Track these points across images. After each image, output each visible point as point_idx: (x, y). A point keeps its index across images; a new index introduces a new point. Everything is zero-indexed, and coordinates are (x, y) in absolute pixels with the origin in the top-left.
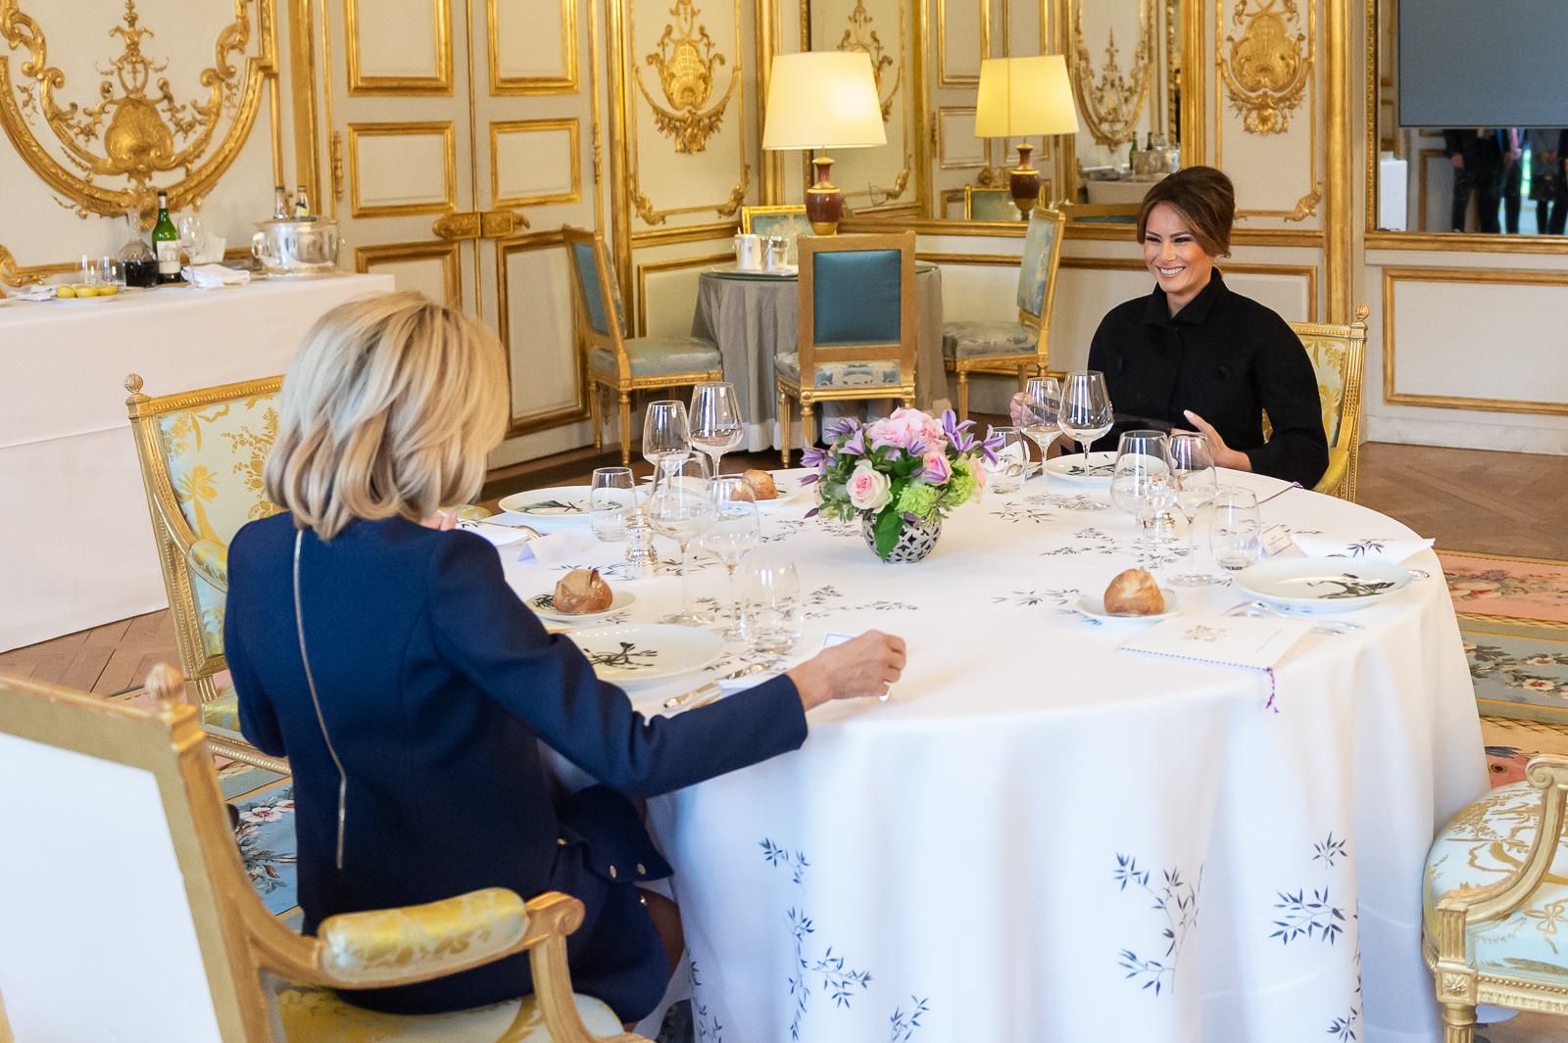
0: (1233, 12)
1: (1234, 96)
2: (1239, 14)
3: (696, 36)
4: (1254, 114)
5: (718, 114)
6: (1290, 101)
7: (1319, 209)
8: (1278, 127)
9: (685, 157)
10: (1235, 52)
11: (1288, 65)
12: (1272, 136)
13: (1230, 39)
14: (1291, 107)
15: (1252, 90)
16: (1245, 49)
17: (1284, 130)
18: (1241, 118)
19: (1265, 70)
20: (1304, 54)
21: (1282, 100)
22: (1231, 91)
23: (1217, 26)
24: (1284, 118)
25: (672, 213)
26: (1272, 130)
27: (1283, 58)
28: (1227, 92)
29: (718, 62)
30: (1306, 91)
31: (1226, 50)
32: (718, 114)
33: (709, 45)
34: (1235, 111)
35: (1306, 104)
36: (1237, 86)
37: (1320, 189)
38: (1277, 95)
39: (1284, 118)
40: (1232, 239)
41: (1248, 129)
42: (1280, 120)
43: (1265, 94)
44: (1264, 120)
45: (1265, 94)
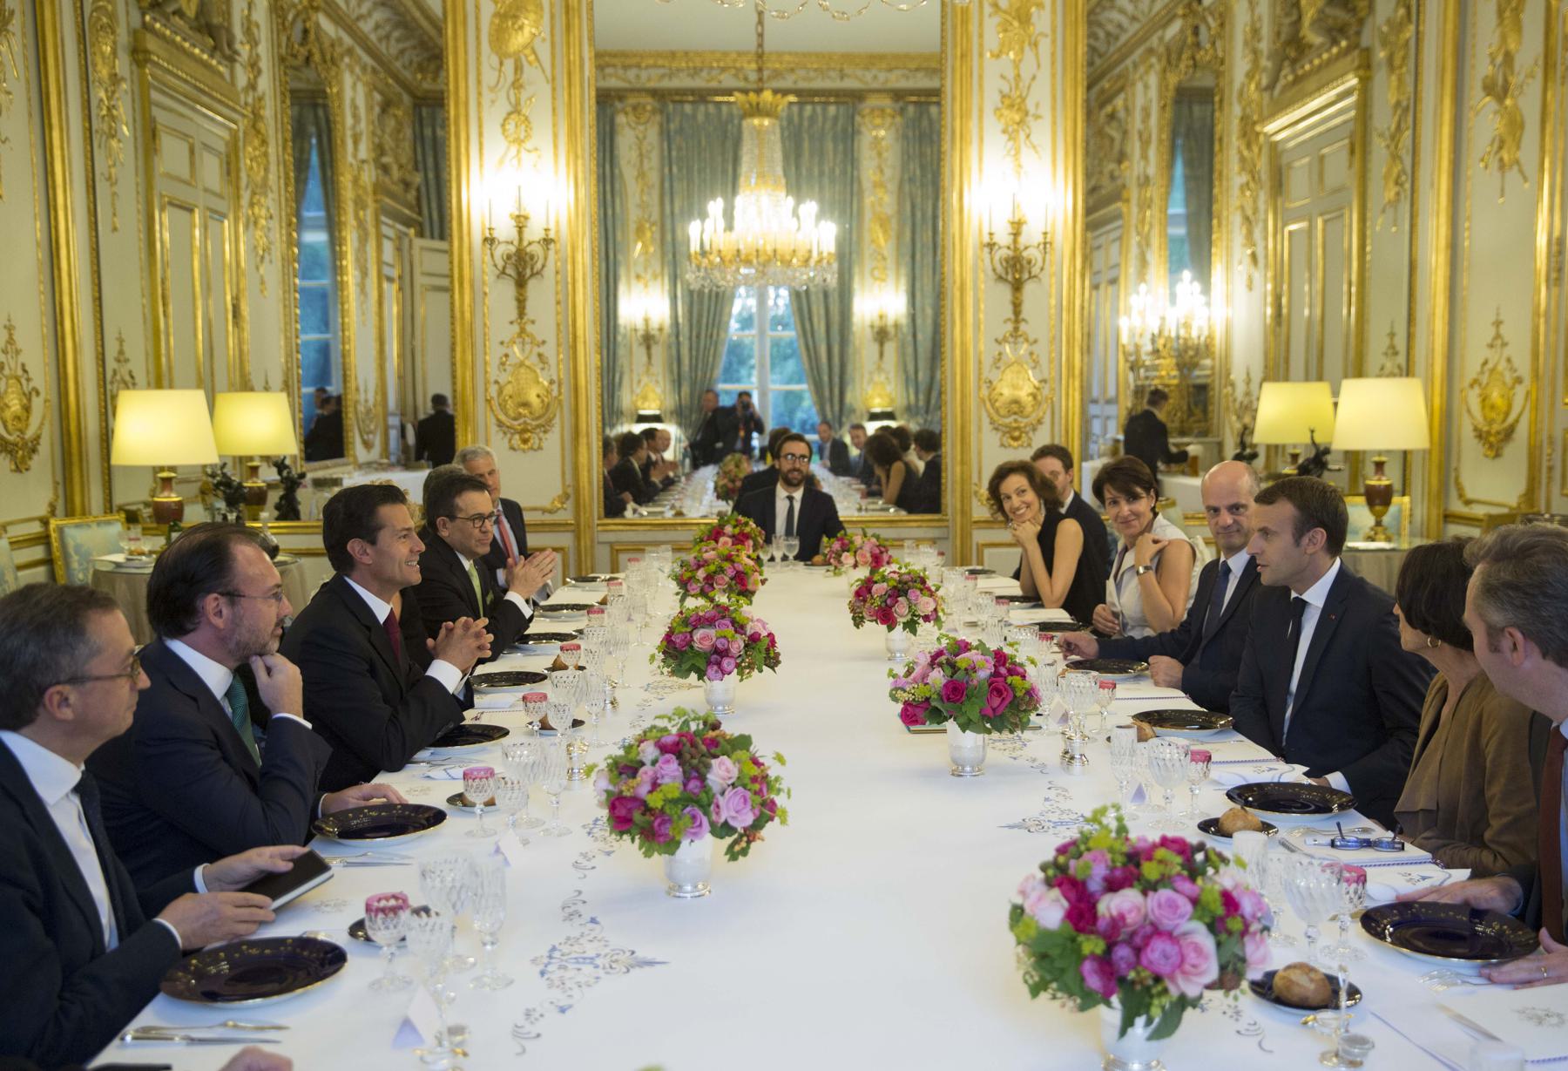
0: (497, 362)
1: (500, 424)
2: (503, 364)
3: (20, 372)
4: (517, 437)
5: (37, 438)
6: (545, 427)
7: (569, 505)
8: (536, 446)
9: (17, 475)
10: (500, 392)
11: (543, 401)
12: (531, 453)
13: (496, 382)
14: (545, 432)
15: (515, 419)
16: (508, 390)
17: (540, 448)
18: (506, 440)
19: (526, 405)
20: (555, 393)
21: (538, 426)
22: (498, 420)
23: (486, 372)
24: (540, 439)
25: (11, 523)
26: (532, 449)
27: (538, 396)
28: (494, 421)
29: (34, 394)
30: (557, 421)
31: (493, 390)
32: (37, 438)
33: (28, 380)
34: (501, 435)
35: (556, 429)
36: (502, 417)
37: (570, 491)
38: (534, 423)
39: (540, 439)
40: (527, 529)
41: (512, 448)
42: (537, 441)
43: (525, 422)
44: (525, 441)
45: (525, 422)
